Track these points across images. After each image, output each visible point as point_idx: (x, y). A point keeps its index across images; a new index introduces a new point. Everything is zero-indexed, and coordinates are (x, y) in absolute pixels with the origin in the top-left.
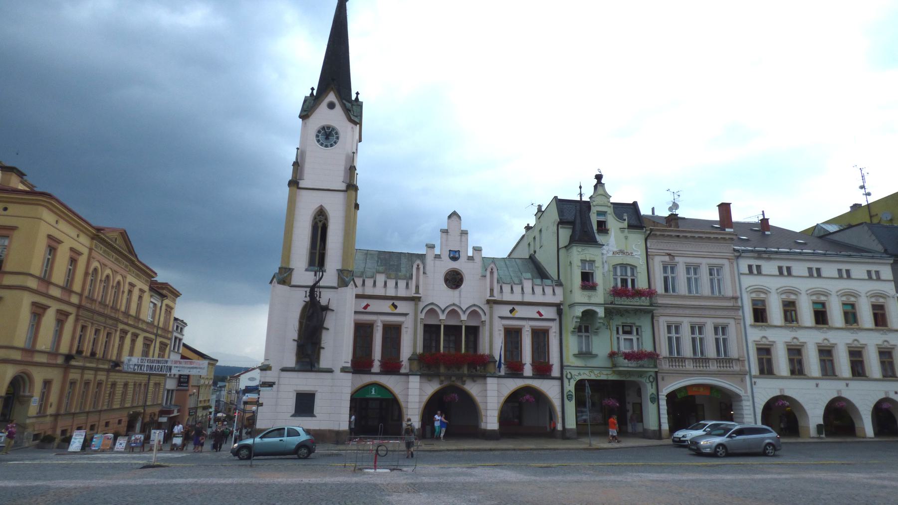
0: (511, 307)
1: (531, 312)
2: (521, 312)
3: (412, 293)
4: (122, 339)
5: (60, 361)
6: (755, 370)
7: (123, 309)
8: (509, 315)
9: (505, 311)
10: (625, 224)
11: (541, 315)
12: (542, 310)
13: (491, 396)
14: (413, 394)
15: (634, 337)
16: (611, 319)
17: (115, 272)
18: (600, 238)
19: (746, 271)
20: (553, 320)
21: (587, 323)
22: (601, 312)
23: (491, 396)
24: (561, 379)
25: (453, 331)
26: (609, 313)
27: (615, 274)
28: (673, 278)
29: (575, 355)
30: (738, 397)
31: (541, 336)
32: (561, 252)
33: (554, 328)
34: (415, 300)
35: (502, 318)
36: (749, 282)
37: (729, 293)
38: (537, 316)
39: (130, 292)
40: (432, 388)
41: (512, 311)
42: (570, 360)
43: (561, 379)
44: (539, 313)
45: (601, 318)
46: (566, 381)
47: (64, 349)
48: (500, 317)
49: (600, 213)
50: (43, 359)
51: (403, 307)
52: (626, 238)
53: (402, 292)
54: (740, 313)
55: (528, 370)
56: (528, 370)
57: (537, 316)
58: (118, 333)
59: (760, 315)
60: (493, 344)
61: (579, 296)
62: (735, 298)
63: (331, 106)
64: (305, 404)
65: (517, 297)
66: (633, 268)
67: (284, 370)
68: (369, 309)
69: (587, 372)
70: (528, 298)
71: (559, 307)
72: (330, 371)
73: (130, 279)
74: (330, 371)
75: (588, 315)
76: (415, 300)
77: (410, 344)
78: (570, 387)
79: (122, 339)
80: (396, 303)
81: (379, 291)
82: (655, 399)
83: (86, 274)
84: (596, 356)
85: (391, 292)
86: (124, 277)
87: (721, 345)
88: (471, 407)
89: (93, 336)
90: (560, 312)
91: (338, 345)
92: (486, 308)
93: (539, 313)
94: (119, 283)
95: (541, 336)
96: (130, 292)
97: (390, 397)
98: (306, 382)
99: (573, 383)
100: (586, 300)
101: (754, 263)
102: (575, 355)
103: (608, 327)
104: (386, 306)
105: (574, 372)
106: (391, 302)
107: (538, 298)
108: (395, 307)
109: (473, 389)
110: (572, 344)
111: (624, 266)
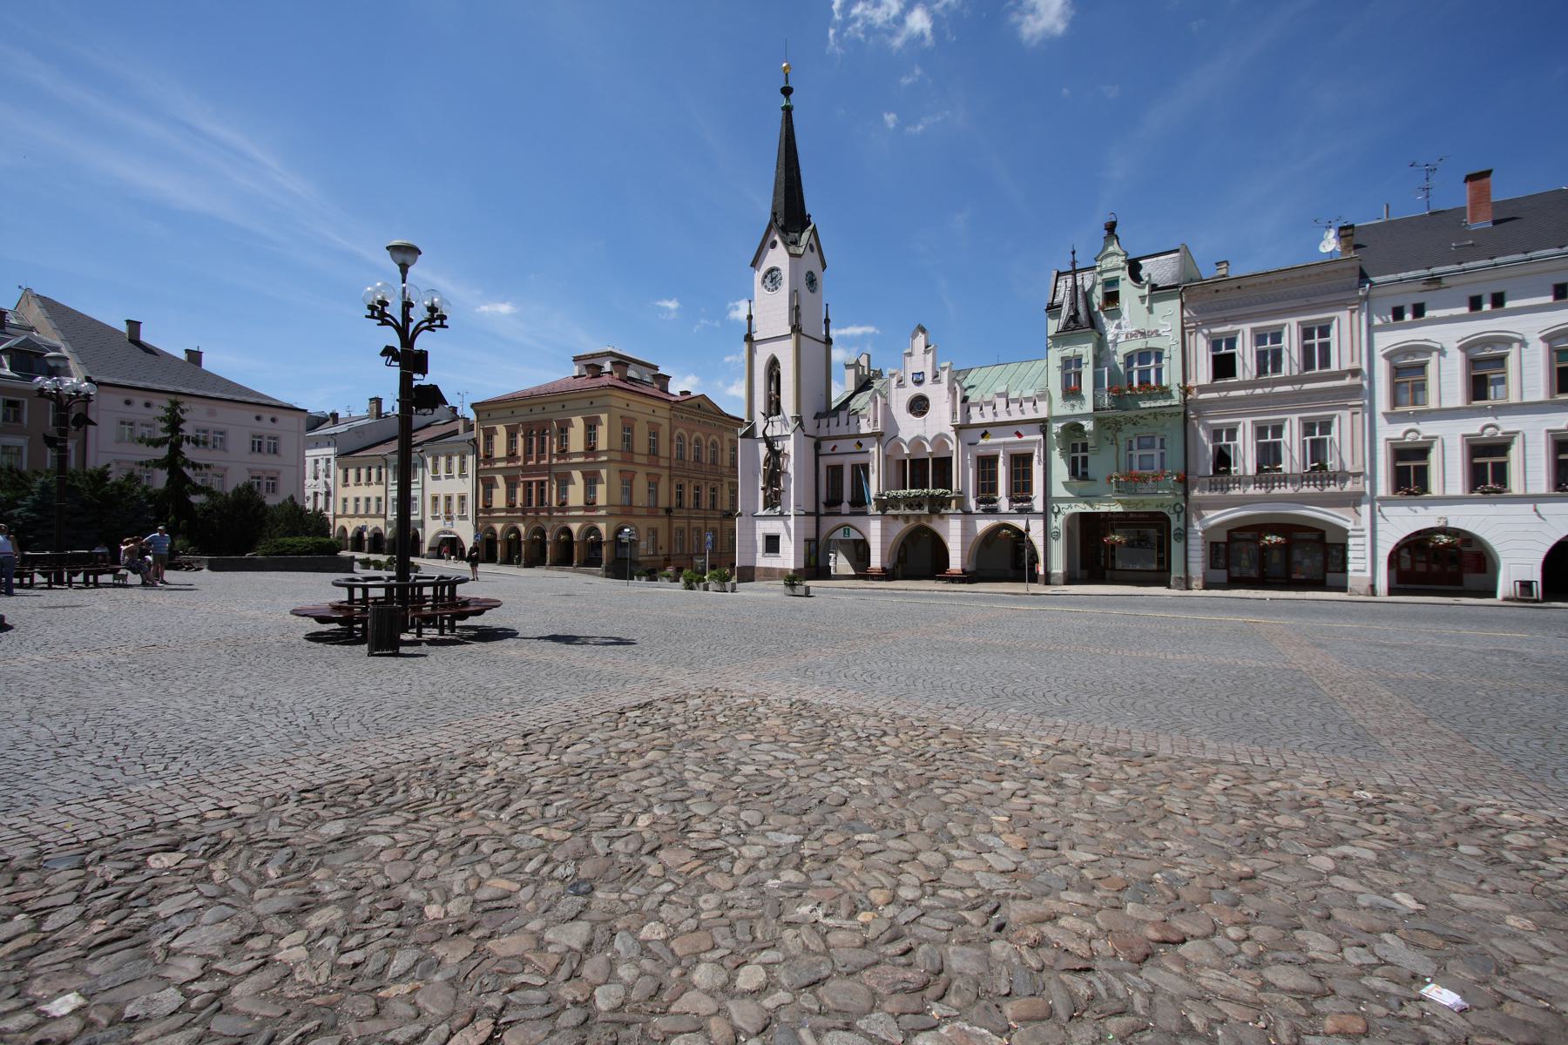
0: (982, 431)
5: (662, 513)
6: (1383, 487)
16: (1119, 430)
22: (1088, 426)
25: (919, 465)
30: (1344, 532)
36: (1388, 340)
37: (1347, 366)
42: (1058, 490)
45: (1090, 433)
47: (663, 501)
50: (644, 512)
58: (726, 486)
60: (964, 477)
62: (1355, 373)
63: (774, 245)
65: (989, 418)
66: (1159, 355)
70: (1003, 417)
71: (1043, 425)
75: (1073, 429)
78: (1058, 523)
82: (1184, 535)
83: (671, 441)
86: (721, 437)
87: (1317, 450)
94: (714, 444)
95: (1021, 464)
98: (774, 527)
99: (1061, 518)
108: (860, 445)
109: (936, 525)
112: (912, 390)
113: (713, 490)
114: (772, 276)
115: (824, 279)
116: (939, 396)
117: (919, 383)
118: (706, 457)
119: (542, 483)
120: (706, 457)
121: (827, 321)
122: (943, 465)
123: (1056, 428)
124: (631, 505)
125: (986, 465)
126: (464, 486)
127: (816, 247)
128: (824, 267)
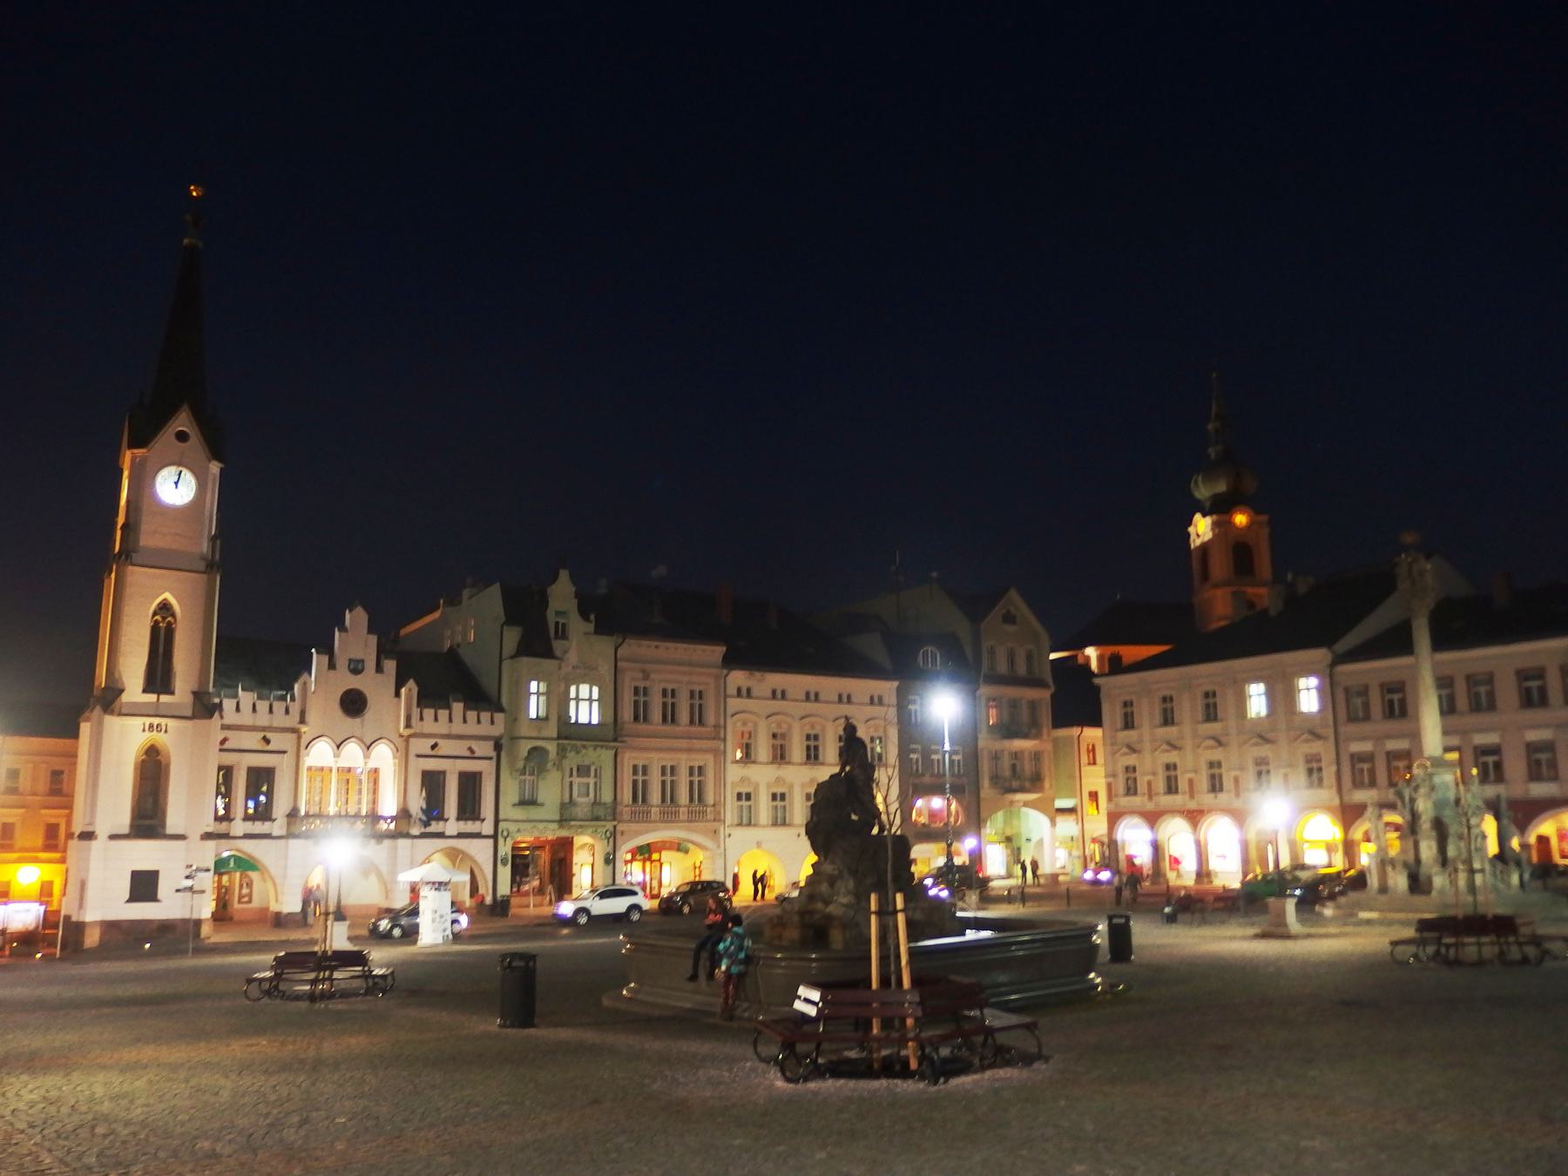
0: (432, 742)
10: (591, 627)
12: (475, 745)
15: (591, 781)
18: (558, 646)
19: (735, 692)
24: (495, 837)
28: (644, 782)
32: (506, 664)
33: (486, 768)
38: (468, 754)
41: (434, 747)
43: (495, 837)
44: (470, 749)
46: (501, 840)
48: (418, 756)
49: (558, 613)
57: (468, 754)
64: (144, 886)
67: (113, 837)
72: (181, 837)
74: (181, 837)
78: (505, 849)
80: (269, 735)
81: (246, 718)
85: (263, 718)
90: (498, 747)
93: (470, 749)
98: (145, 854)
100: (534, 734)
103: (559, 767)
104: (252, 740)
105: (512, 827)
106: (262, 734)
108: (267, 741)
112: (346, 681)
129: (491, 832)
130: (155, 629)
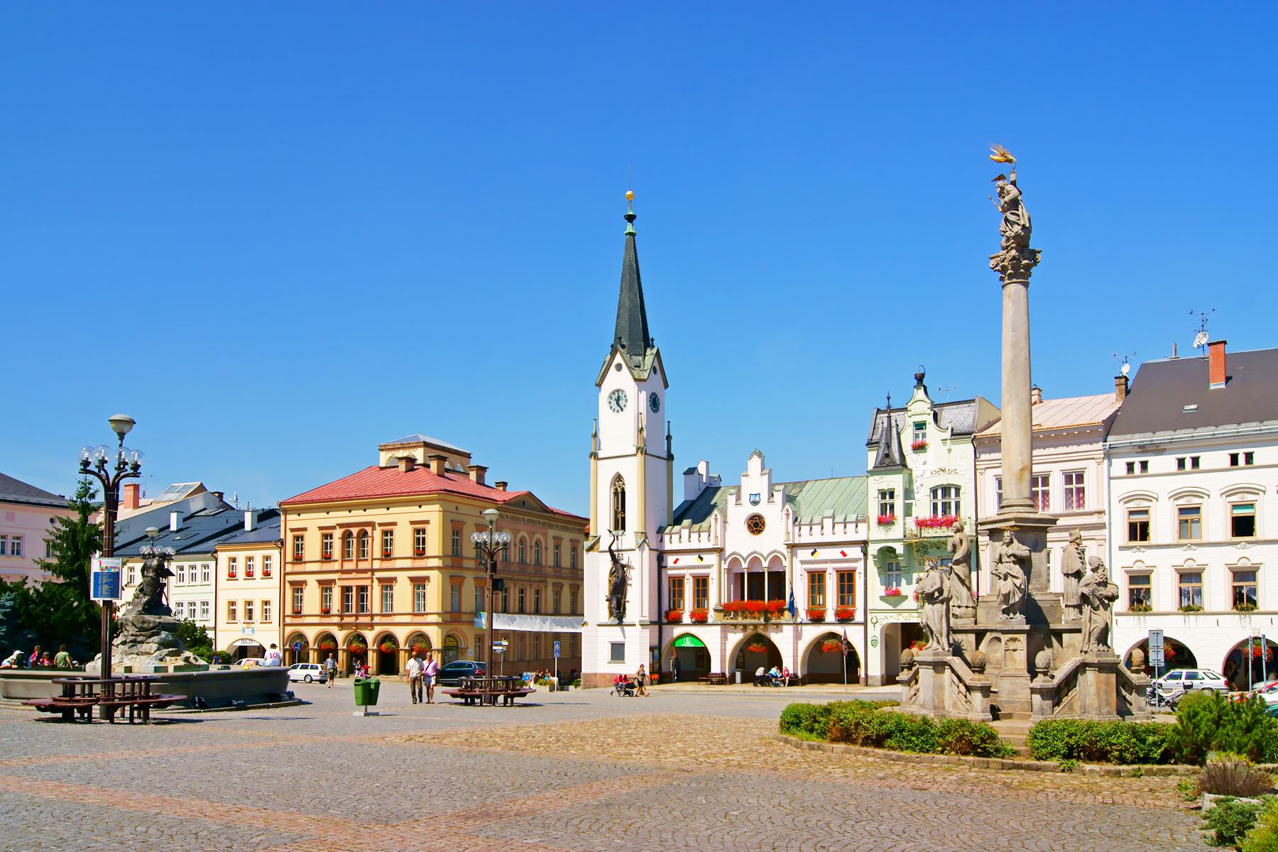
1: (835, 553)
2: (823, 553)
3: (710, 545)
4: (558, 594)
7: (551, 563)
8: (811, 558)
9: (804, 554)
11: (844, 555)
12: (846, 550)
13: (792, 643)
14: (719, 643)
16: (926, 552)
17: (532, 534)
20: (856, 560)
21: (888, 561)
22: (900, 549)
23: (792, 643)
25: (756, 578)
26: (909, 547)
27: (935, 496)
29: (882, 598)
31: (846, 579)
34: (720, 551)
35: (803, 562)
37: (1093, 509)
38: (841, 557)
39: (557, 547)
40: (735, 638)
42: (875, 602)
43: (865, 624)
51: (711, 559)
52: (950, 451)
53: (705, 544)
54: (1106, 532)
55: (830, 616)
56: (830, 616)
58: (550, 588)
59: (1139, 531)
60: (798, 588)
61: (877, 533)
63: (619, 367)
65: (816, 538)
68: (679, 563)
69: (895, 615)
71: (864, 544)
73: (552, 533)
76: (720, 551)
77: (717, 594)
79: (558, 594)
81: (685, 545)
84: (906, 597)
86: (545, 535)
88: (774, 657)
89: (533, 596)
91: (639, 601)
92: (785, 550)
95: (846, 579)
96: (557, 547)
97: (701, 645)
101: (1137, 460)
102: (882, 598)
104: (692, 560)
107: (840, 537)
108: (701, 559)
109: (775, 637)
110: (877, 588)
111: (946, 490)
113: (538, 592)
114: (618, 399)
115: (667, 398)
116: (773, 513)
117: (755, 503)
118: (530, 558)
119: (363, 589)
120: (530, 558)
121: (669, 438)
122: (778, 579)
123: (873, 549)
124: (459, 611)
125: (816, 579)
126: (267, 590)
127: (658, 368)
128: (666, 386)
129: (862, 620)
130: (616, 494)
